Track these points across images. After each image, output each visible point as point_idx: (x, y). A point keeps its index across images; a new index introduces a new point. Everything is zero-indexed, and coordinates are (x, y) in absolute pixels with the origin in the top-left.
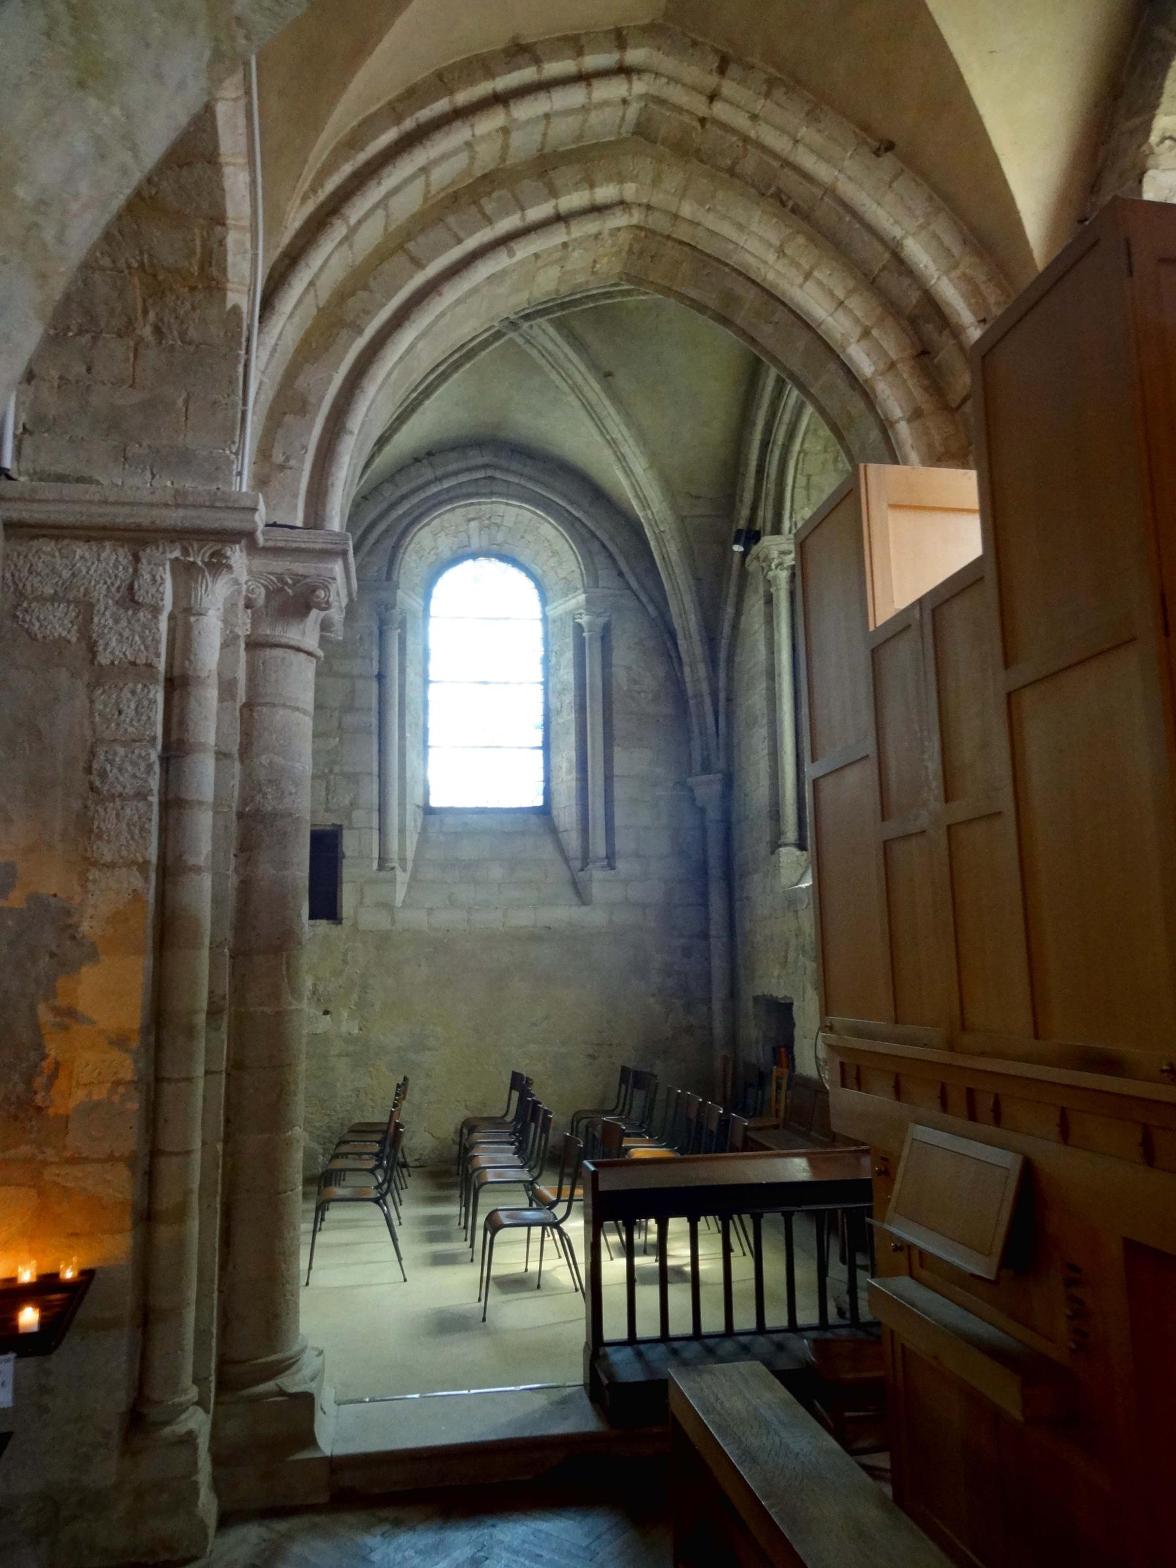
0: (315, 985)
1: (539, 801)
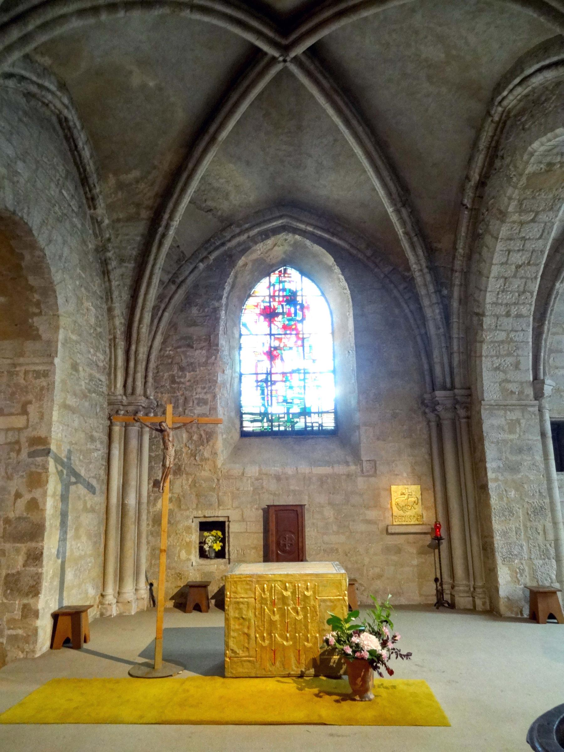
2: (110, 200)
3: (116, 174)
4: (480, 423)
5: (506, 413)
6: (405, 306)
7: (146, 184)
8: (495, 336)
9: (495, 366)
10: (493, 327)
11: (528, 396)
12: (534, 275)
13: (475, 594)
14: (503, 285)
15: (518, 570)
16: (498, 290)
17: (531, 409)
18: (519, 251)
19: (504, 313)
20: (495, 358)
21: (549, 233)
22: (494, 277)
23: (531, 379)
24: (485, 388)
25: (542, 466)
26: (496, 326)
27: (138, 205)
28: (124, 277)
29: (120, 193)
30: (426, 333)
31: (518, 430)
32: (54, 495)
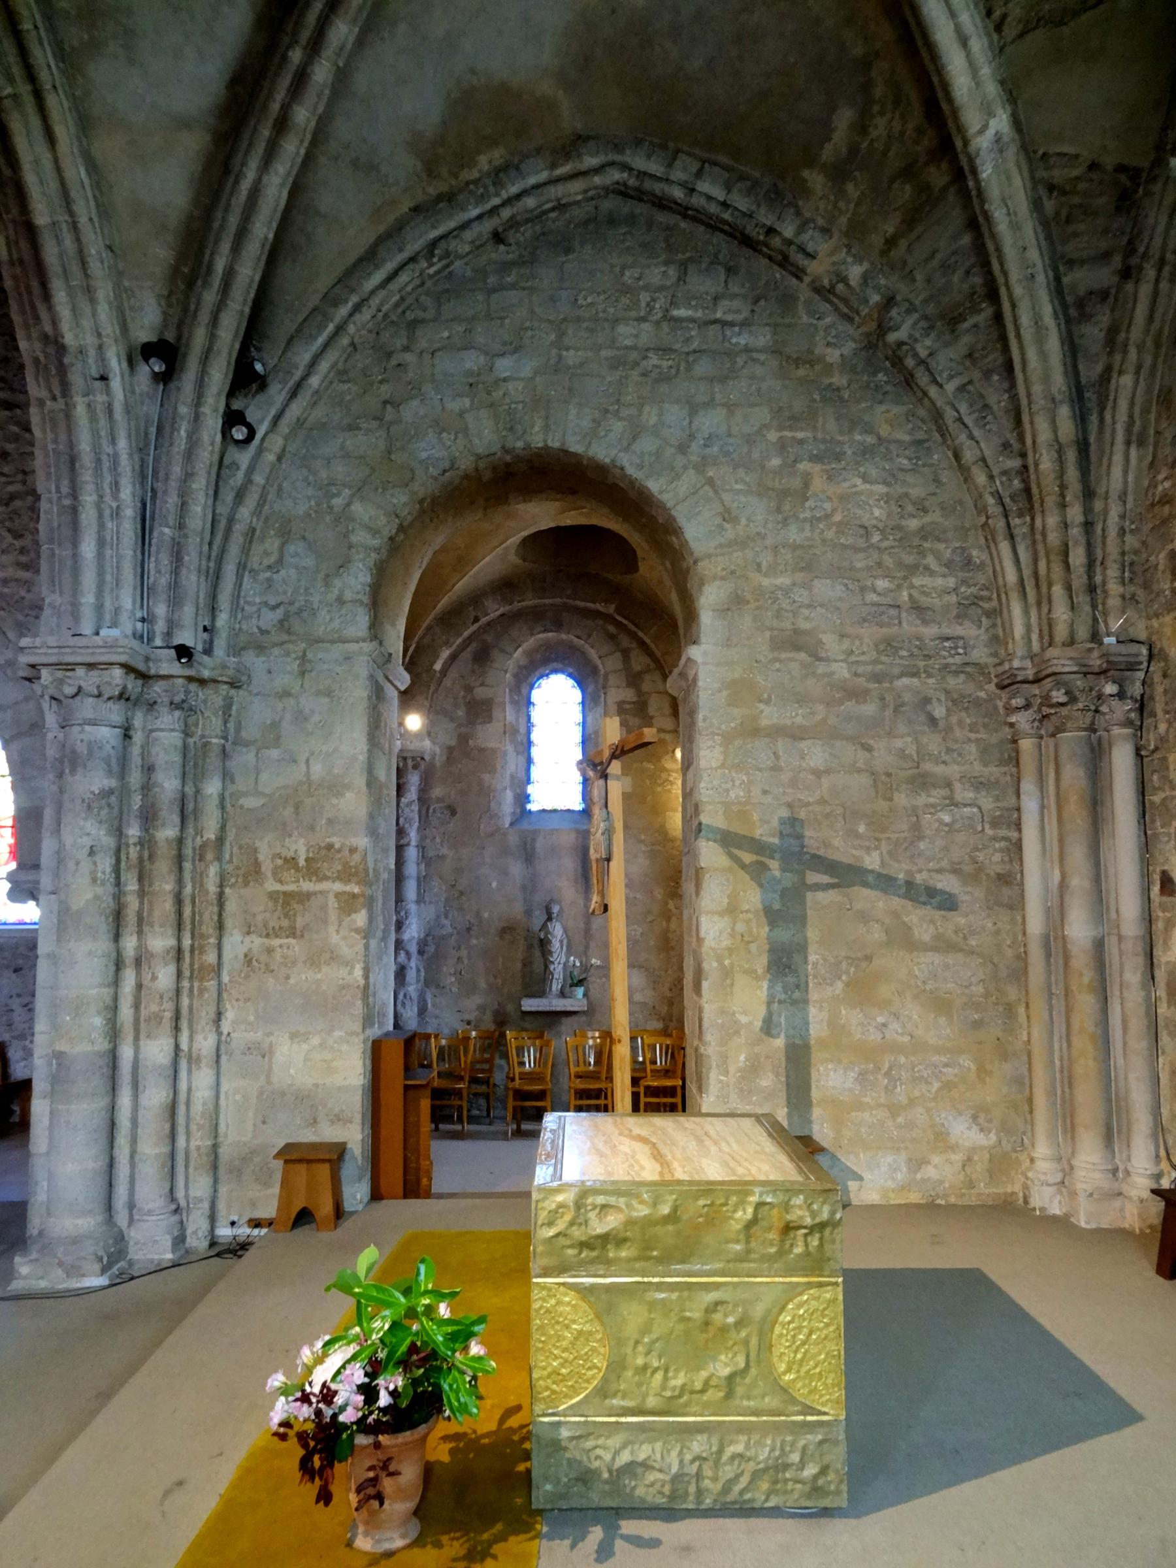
2: (843, 221)
3: (810, 161)
7: (882, 113)
27: (908, 172)
28: (977, 355)
29: (850, 187)
32: (732, 910)
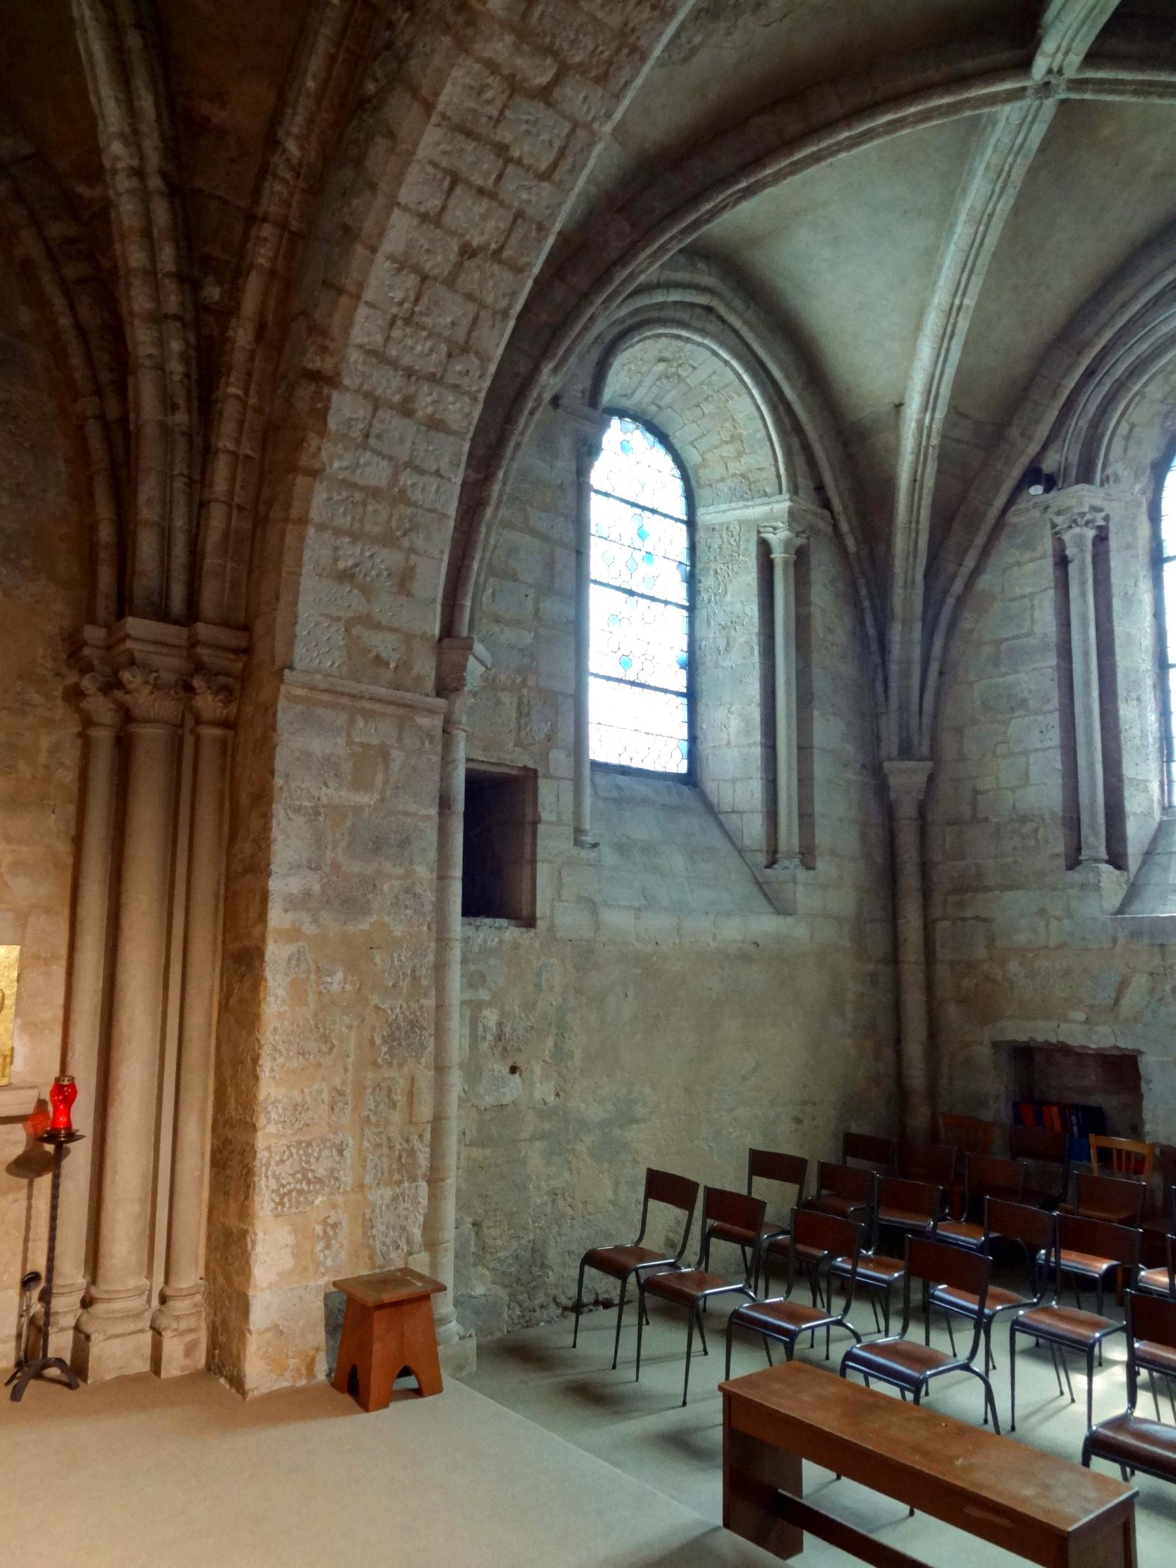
0: (500, 1024)
1: (683, 768)
4: (266, 747)
5: (352, 722)
6: (59, 303)
8: (358, 465)
9: (341, 565)
10: (356, 433)
11: (419, 679)
12: (503, 303)
13: (163, 1322)
14: (412, 298)
15: (319, 1229)
16: (395, 310)
17: (425, 721)
18: (481, 191)
19: (397, 398)
20: (347, 540)
21: (574, 170)
22: (392, 258)
23: (437, 632)
24: (302, 630)
25: (429, 897)
26: (367, 436)
30: (124, 420)
31: (380, 777)
